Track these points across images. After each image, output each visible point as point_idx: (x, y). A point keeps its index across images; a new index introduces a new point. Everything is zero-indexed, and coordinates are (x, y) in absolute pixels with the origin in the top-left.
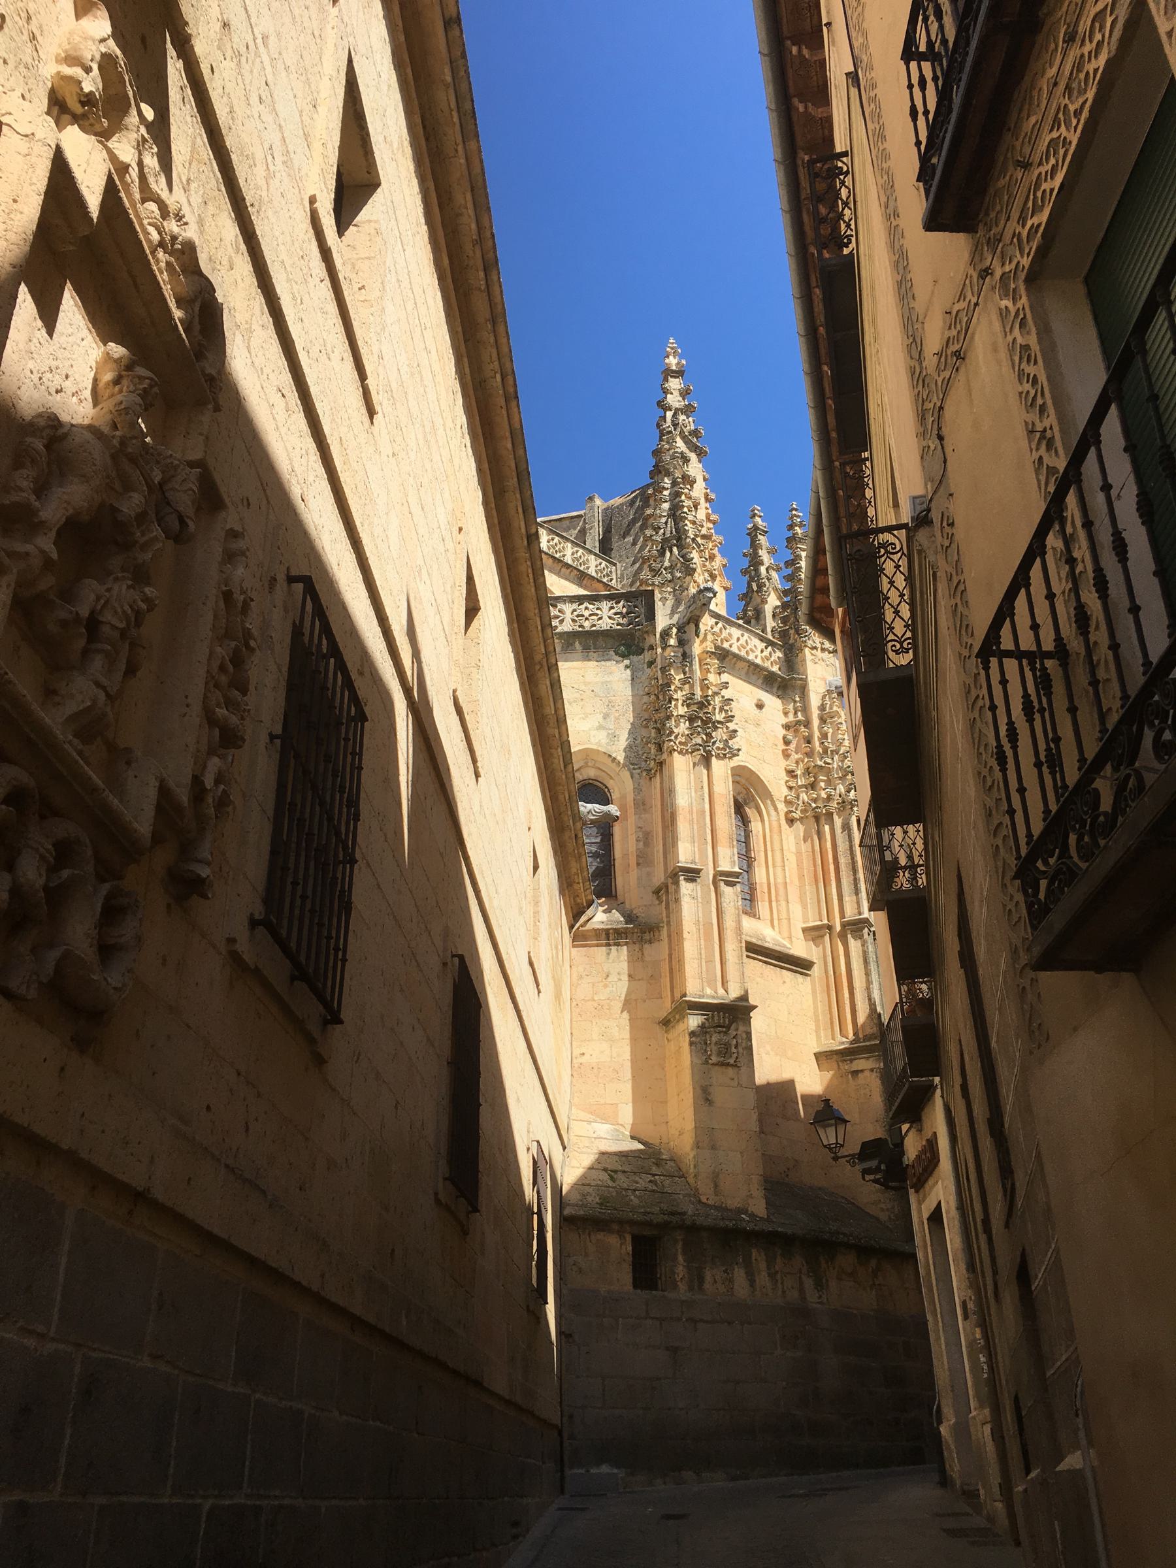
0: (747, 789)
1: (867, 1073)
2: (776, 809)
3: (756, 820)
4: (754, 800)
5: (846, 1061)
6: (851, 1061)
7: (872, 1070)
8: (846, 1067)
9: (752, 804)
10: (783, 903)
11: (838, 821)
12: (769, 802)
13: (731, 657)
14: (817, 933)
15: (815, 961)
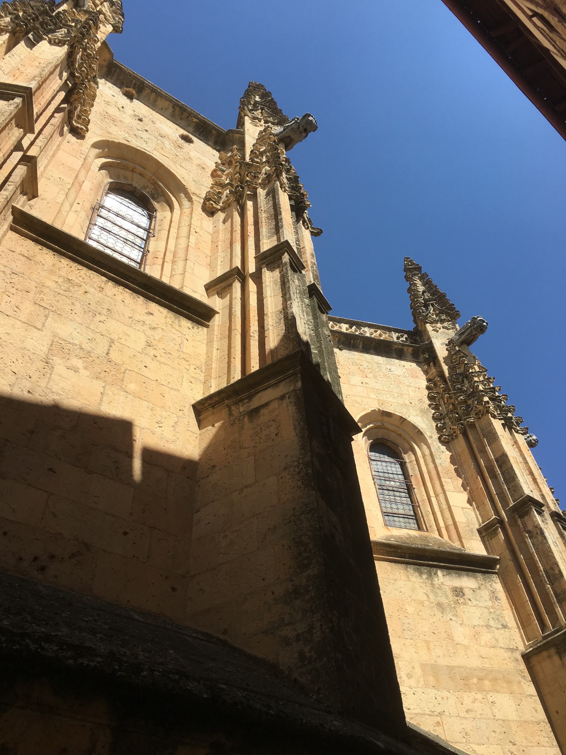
0: (155, 184)
1: (275, 405)
2: (190, 200)
3: (163, 210)
4: (164, 195)
5: (241, 401)
6: (250, 398)
7: (282, 398)
8: (242, 409)
9: (161, 198)
10: (180, 264)
11: (261, 193)
12: (182, 195)
13: (147, 91)
14: (223, 285)
15: (217, 309)
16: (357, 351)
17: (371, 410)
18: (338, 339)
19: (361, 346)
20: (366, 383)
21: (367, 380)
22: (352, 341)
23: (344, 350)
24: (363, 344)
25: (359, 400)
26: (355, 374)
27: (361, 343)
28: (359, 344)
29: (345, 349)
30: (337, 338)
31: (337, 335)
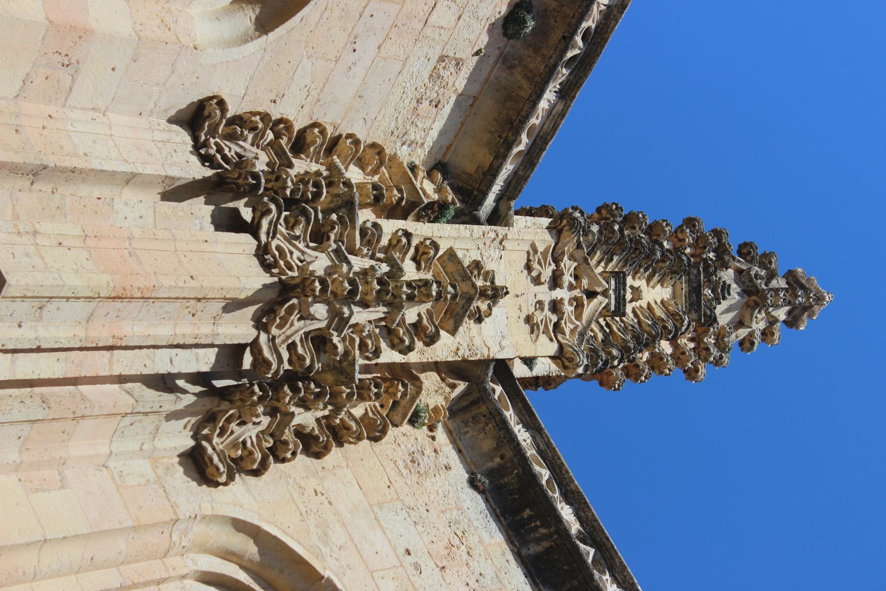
16: (510, 541)
17: (329, 580)
18: (500, 465)
19: (533, 549)
20: (417, 567)
21: (428, 567)
22: (527, 513)
23: (479, 498)
24: (547, 551)
25: (338, 536)
26: (419, 527)
27: (545, 544)
28: (538, 541)
29: (487, 501)
30: (498, 460)
31: (509, 454)
